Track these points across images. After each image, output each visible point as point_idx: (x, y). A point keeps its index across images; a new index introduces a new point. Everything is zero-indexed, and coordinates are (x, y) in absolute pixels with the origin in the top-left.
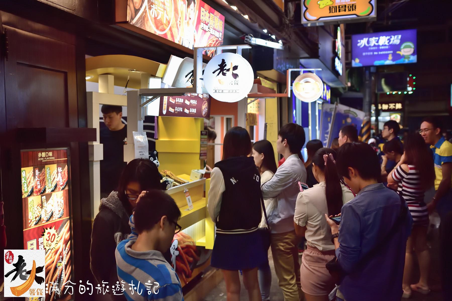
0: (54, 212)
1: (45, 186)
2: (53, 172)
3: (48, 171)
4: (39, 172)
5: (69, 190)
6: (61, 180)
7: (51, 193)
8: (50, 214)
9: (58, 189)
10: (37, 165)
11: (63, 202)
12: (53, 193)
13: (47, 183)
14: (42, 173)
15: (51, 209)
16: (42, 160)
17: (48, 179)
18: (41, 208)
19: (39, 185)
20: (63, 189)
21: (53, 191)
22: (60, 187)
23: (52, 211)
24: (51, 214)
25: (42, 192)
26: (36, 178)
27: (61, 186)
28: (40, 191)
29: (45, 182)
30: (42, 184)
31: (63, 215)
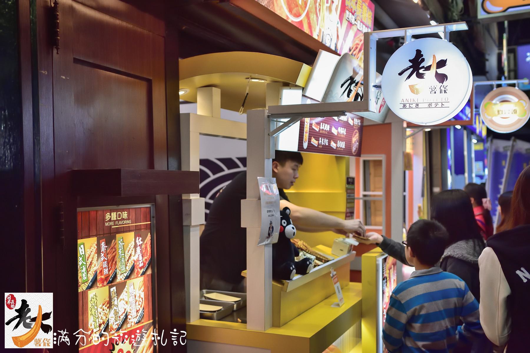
0: (130, 314)
1: (116, 270)
2: (128, 245)
3: (121, 244)
4: (107, 247)
5: (152, 275)
6: (141, 258)
7: (125, 280)
8: (123, 317)
9: (135, 274)
10: (104, 234)
11: (143, 296)
12: (129, 282)
13: (119, 264)
14: (111, 248)
15: (125, 309)
16: (111, 226)
17: (121, 257)
18: (108, 308)
19: (106, 268)
20: (144, 273)
21: (128, 277)
22: (139, 270)
23: (127, 312)
24: (125, 317)
25: (111, 280)
26: (102, 256)
27: (141, 268)
28: (106, 278)
29: (116, 262)
30: (111, 266)
31: (142, 317)
